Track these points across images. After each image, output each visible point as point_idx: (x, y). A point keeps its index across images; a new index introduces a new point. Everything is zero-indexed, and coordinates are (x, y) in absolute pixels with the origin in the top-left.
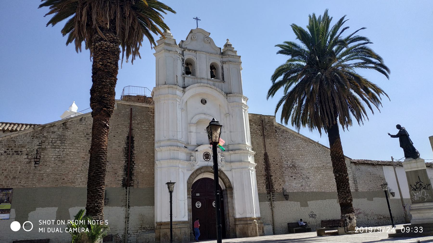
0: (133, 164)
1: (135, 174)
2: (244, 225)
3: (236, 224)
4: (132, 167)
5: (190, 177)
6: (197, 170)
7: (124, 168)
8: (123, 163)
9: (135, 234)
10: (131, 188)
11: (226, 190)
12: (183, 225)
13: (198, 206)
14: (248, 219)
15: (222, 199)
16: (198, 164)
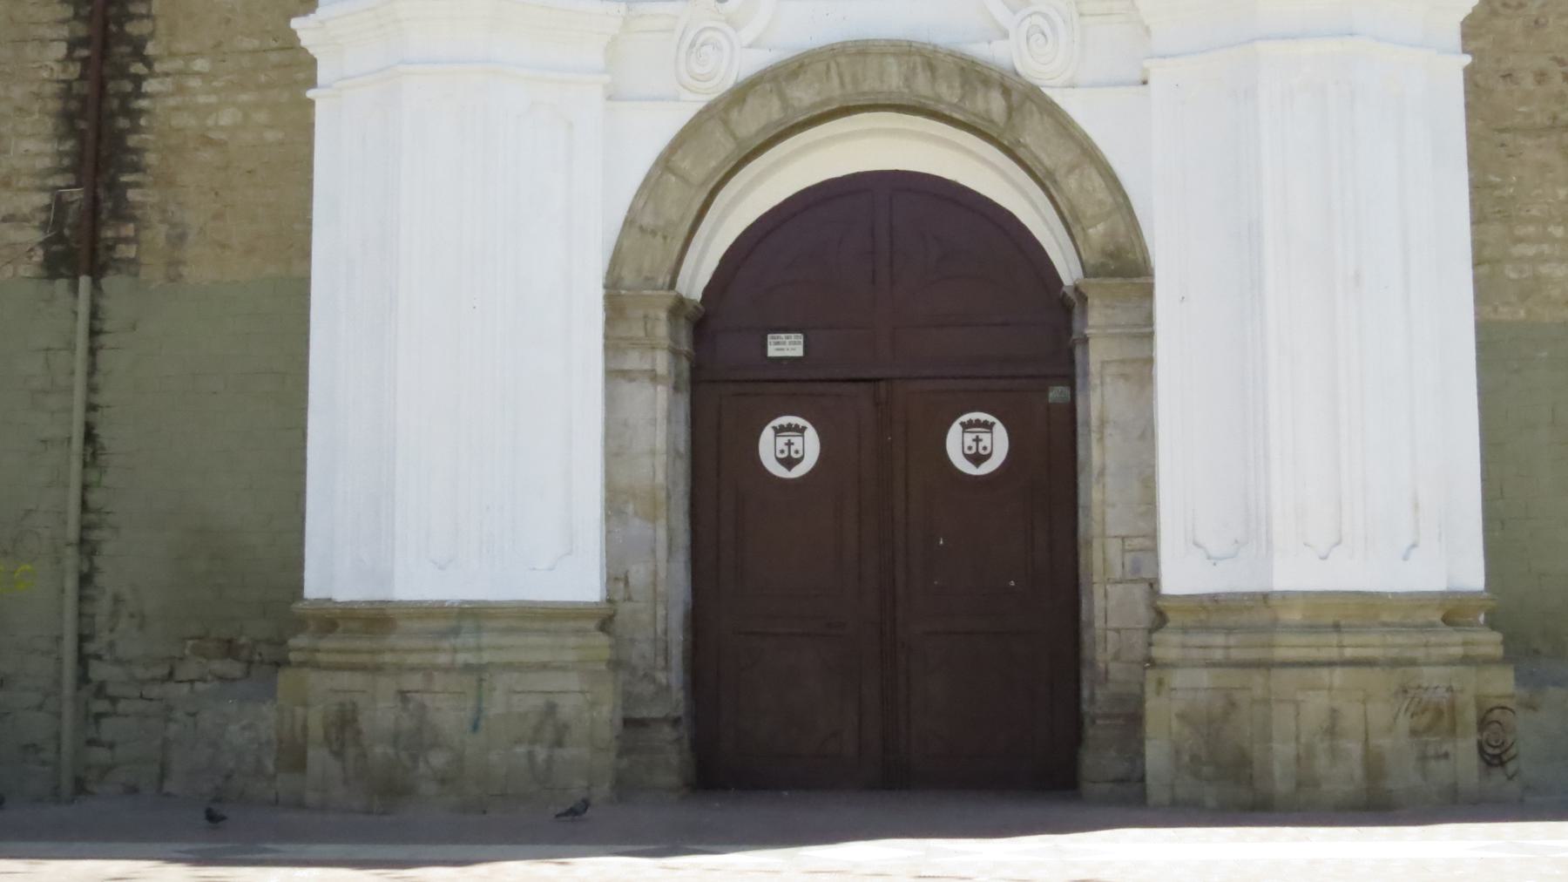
0: (138, 68)
1: (151, 158)
2: (1234, 678)
3: (1151, 662)
4: (125, 98)
5: (665, 163)
6: (740, 94)
7: (54, 105)
8: (50, 61)
9: (155, 691)
10: (110, 282)
11: (1083, 299)
12: (535, 647)
13: (789, 463)
14: (1295, 616)
15: (1057, 394)
16: (747, 35)
